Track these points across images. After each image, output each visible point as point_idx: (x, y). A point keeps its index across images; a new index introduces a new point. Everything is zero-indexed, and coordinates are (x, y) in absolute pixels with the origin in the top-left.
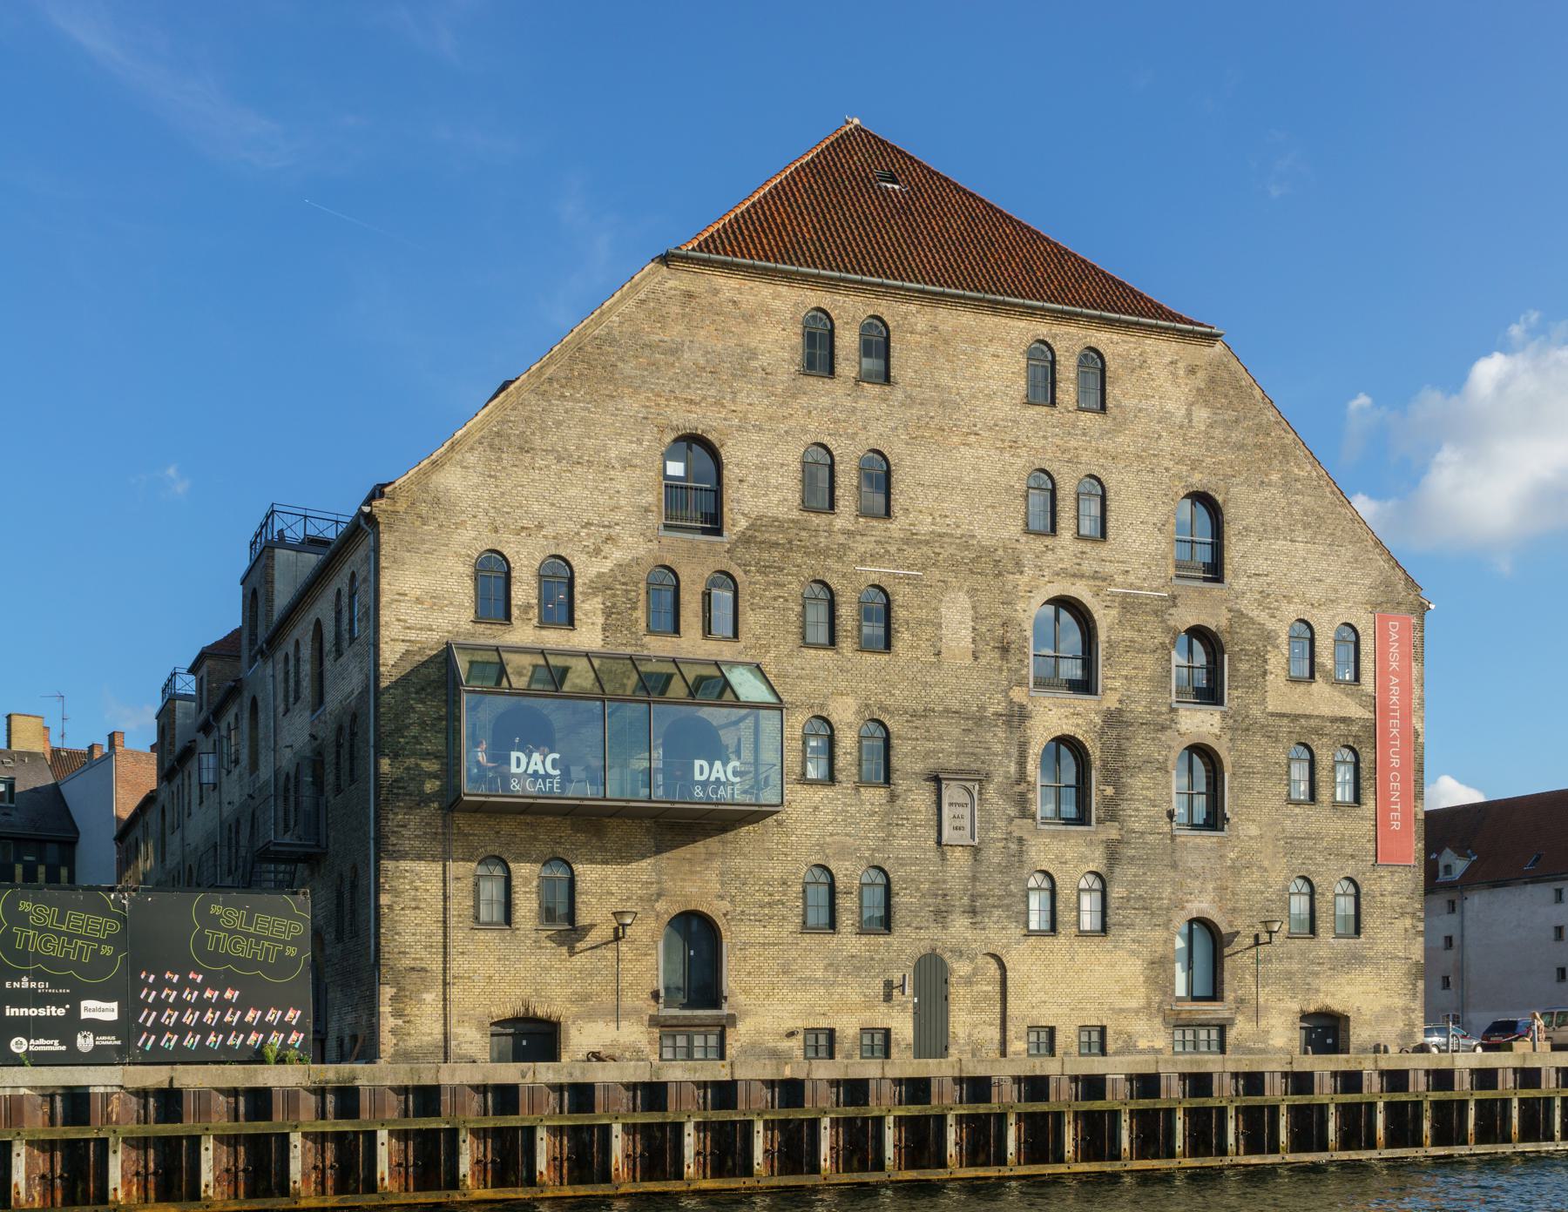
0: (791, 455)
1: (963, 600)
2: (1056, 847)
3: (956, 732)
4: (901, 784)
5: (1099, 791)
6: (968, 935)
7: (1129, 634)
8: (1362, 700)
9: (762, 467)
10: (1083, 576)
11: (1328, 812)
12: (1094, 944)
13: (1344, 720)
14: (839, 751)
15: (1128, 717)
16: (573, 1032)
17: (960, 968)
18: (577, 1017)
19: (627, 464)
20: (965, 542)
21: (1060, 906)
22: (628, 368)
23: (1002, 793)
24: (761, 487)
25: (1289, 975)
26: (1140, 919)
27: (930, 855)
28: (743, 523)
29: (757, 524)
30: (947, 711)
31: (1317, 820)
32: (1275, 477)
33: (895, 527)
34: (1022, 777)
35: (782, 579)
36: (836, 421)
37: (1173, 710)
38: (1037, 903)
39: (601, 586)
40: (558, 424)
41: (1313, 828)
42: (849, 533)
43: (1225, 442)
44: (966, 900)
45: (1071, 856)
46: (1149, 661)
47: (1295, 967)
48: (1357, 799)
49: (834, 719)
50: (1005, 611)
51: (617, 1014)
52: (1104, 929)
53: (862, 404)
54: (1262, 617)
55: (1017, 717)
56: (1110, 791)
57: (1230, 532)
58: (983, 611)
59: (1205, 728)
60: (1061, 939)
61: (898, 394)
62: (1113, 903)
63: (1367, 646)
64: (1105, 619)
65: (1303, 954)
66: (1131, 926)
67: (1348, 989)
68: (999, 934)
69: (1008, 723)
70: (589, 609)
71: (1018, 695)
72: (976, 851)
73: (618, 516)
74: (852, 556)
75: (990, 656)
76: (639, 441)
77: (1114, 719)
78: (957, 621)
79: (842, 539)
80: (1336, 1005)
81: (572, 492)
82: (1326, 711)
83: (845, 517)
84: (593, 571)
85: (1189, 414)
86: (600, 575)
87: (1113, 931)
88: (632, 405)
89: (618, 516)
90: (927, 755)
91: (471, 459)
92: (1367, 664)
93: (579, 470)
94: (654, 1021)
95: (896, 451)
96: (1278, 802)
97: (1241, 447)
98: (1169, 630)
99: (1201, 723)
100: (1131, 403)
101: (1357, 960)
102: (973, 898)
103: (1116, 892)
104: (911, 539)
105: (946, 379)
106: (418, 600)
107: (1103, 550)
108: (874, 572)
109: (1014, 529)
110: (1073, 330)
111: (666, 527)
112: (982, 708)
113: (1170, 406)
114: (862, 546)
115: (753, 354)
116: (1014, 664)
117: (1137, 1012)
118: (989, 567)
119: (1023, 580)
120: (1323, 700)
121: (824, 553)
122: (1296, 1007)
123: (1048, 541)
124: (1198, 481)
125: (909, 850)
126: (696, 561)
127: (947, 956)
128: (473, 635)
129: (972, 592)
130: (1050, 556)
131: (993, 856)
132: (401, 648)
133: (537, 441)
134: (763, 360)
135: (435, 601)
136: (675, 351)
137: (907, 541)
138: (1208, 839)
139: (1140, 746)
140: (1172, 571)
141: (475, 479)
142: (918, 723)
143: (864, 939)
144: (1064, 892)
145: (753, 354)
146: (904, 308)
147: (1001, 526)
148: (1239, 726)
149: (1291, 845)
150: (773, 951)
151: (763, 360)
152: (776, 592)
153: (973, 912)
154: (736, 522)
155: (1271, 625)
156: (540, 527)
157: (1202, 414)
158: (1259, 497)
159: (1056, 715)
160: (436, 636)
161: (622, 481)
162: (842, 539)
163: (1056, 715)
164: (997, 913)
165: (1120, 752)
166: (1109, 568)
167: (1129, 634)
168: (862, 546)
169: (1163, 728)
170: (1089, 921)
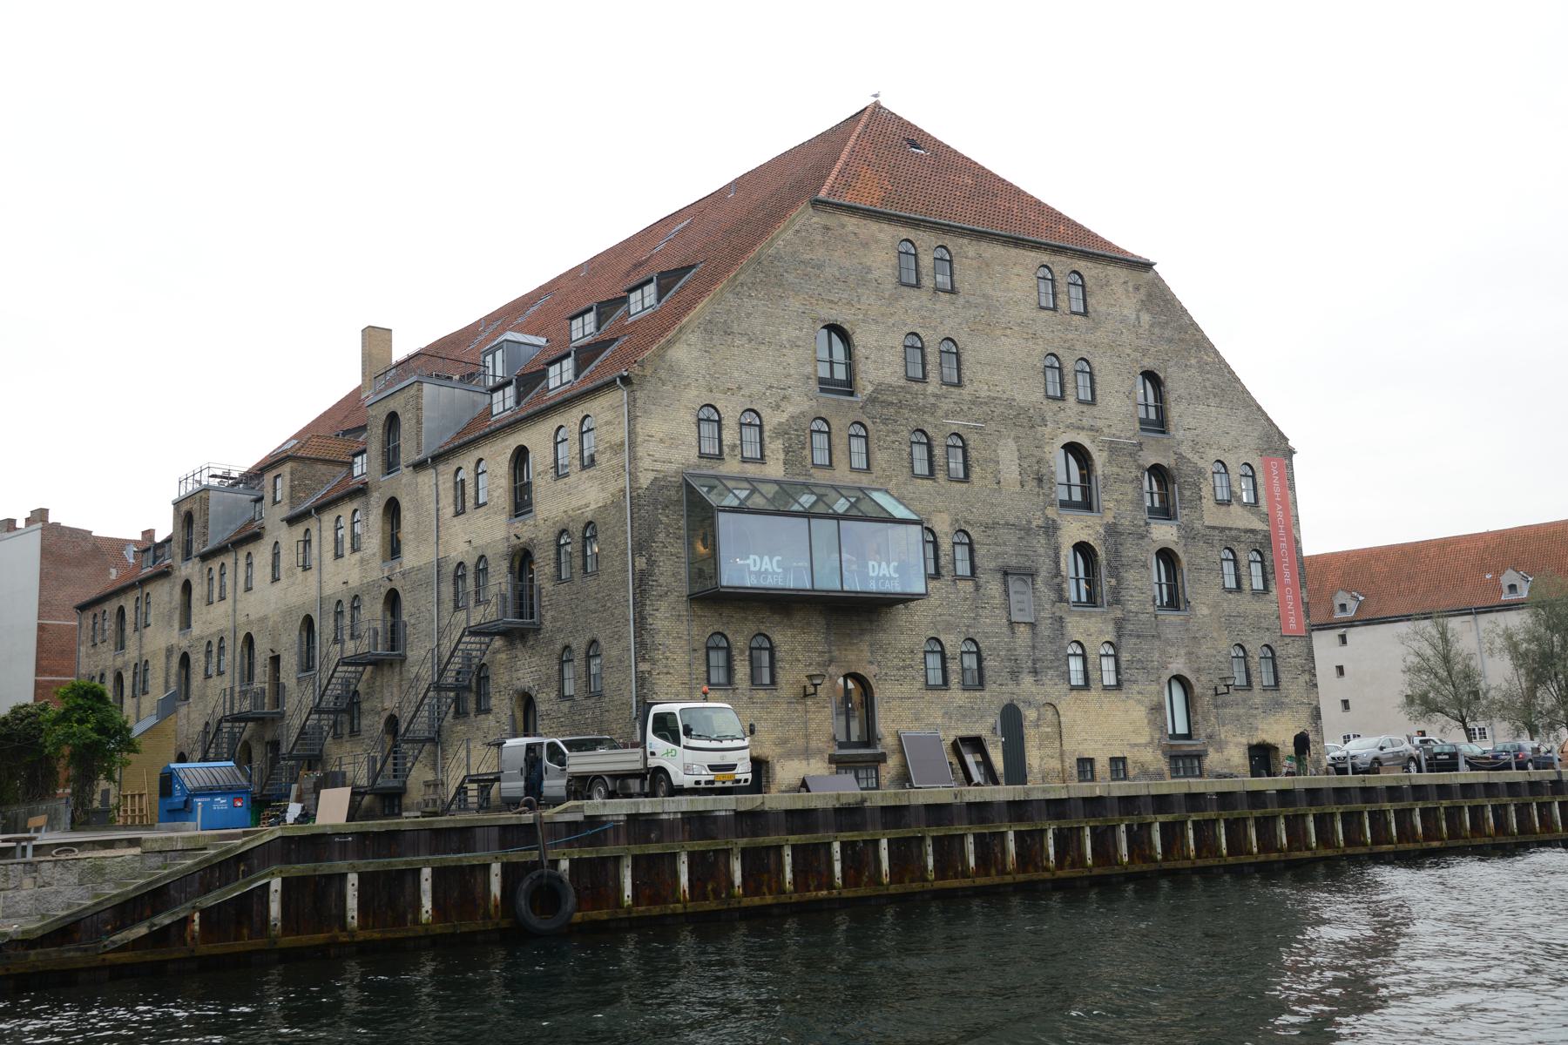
0: (897, 340)
2: (1084, 622)
3: (1014, 540)
4: (983, 578)
5: (1106, 583)
6: (1033, 689)
7: (1115, 470)
8: (1265, 518)
9: (880, 349)
11: (1249, 597)
12: (1113, 696)
13: (1253, 531)
14: (941, 554)
15: (1120, 529)
16: (778, 768)
17: (1030, 715)
18: (781, 756)
19: (794, 345)
20: (1010, 403)
21: (1090, 667)
22: (790, 277)
23: (1046, 584)
24: (880, 366)
25: (1238, 718)
26: (1141, 676)
27: (1005, 629)
28: (870, 388)
30: (1007, 524)
31: (1245, 603)
32: (1193, 361)
33: (966, 392)
34: (1058, 573)
35: (897, 428)
37: (1147, 524)
38: (1075, 665)
39: (781, 432)
40: (749, 315)
41: (1241, 609)
42: (935, 395)
43: (1161, 337)
44: (1030, 664)
45: (1091, 629)
46: (1129, 488)
47: (1242, 711)
48: (1266, 589)
49: (936, 529)
50: (1037, 453)
52: (1119, 685)
53: (938, 306)
54: (1195, 459)
55: (1051, 529)
56: (1113, 582)
57: (1171, 398)
58: (1025, 453)
59: (1168, 537)
60: (1093, 692)
61: (961, 301)
62: (1123, 665)
63: (1260, 479)
64: (1099, 458)
65: (1244, 701)
66: (1135, 682)
67: (1276, 727)
68: (1052, 689)
69: (1046, 533)
70: (775, 448)
71: (1051, 512)
72: (1033, 625)
74: (940, 413)
75: (1031, 484)
76: (801, 329)
77: (1112, 531)
79: (932, 400)
80: (1270, 739)
81: (759, 364)
82: (1240, 524)
83: (933, 386)
84: (776, 421)
85: (1138, 318)
86: (780, 424)
87: (1126, 685)
88: (795, 304)
89: (790, 382)
90: (997, 556)
91: (693, 338)
92: (1261, 492)
93: (763, 348)
94: (833, 759)
95: (962, 339)
96: (1218, 590)
97: (1170, 341)
98: (1139, 467)
99: (1164, 533)
100: (1102, 309)
101: (1278, 705)
102: (1034, 662)
103: (1125, 657)
104: (975, 401)
105: (991, 292)
106: (662, 441)
107: (1095, 411)
108: (955, 424)
109: (1038, 395)
110: (1063, 259)
111: (822, 390)
112: (1029, 522)
113: (1126, 312)
114: (946, 405)
115: (869, 270)
116: (1046, 491)
117: (1146, 745)
118: (1025, 421)
119: (1047, 430)
120: (1238, 518)
121: (921, 410)
122: (1244, 741)
123: (1060, 404)
124: (1149, 364)
125: (990, 625)
126: (842, 414)
127: (1021, 705)
128: (699, 467)
130: (1062, 414)
131: (1045, 630)
132: (651, 475)
133: (735, 328)
134: (876, 274)
135: (672, 441)
138: (1171, 617)
139: (1130, 550)
140: (1138, 426)
141: (696, 354)
142: (990, 532)
143: (967, 694)
144: (1091, 657)
145: (869, 270)
146: (960, 241)
147: (1029, 394)
148: (1189, 535)
149: (1229, 621)
151: (876, 274)
152: (893, 437)
153: (1035, 672)
154: (865, 388)
155: (1201, 464)
156: (740, 388)
157: (1146, 318)
158: (1185, 375)
159: (1076, 528)
160: (674, 467)
161: (791, 357)
162: (932, 400)
163: (1076, 528)
164: (1050, 672)
166: (1099, 424)
167: (1115, 470)
168: (946, 405)
169: (1142, 537)
170: (1109, 679)
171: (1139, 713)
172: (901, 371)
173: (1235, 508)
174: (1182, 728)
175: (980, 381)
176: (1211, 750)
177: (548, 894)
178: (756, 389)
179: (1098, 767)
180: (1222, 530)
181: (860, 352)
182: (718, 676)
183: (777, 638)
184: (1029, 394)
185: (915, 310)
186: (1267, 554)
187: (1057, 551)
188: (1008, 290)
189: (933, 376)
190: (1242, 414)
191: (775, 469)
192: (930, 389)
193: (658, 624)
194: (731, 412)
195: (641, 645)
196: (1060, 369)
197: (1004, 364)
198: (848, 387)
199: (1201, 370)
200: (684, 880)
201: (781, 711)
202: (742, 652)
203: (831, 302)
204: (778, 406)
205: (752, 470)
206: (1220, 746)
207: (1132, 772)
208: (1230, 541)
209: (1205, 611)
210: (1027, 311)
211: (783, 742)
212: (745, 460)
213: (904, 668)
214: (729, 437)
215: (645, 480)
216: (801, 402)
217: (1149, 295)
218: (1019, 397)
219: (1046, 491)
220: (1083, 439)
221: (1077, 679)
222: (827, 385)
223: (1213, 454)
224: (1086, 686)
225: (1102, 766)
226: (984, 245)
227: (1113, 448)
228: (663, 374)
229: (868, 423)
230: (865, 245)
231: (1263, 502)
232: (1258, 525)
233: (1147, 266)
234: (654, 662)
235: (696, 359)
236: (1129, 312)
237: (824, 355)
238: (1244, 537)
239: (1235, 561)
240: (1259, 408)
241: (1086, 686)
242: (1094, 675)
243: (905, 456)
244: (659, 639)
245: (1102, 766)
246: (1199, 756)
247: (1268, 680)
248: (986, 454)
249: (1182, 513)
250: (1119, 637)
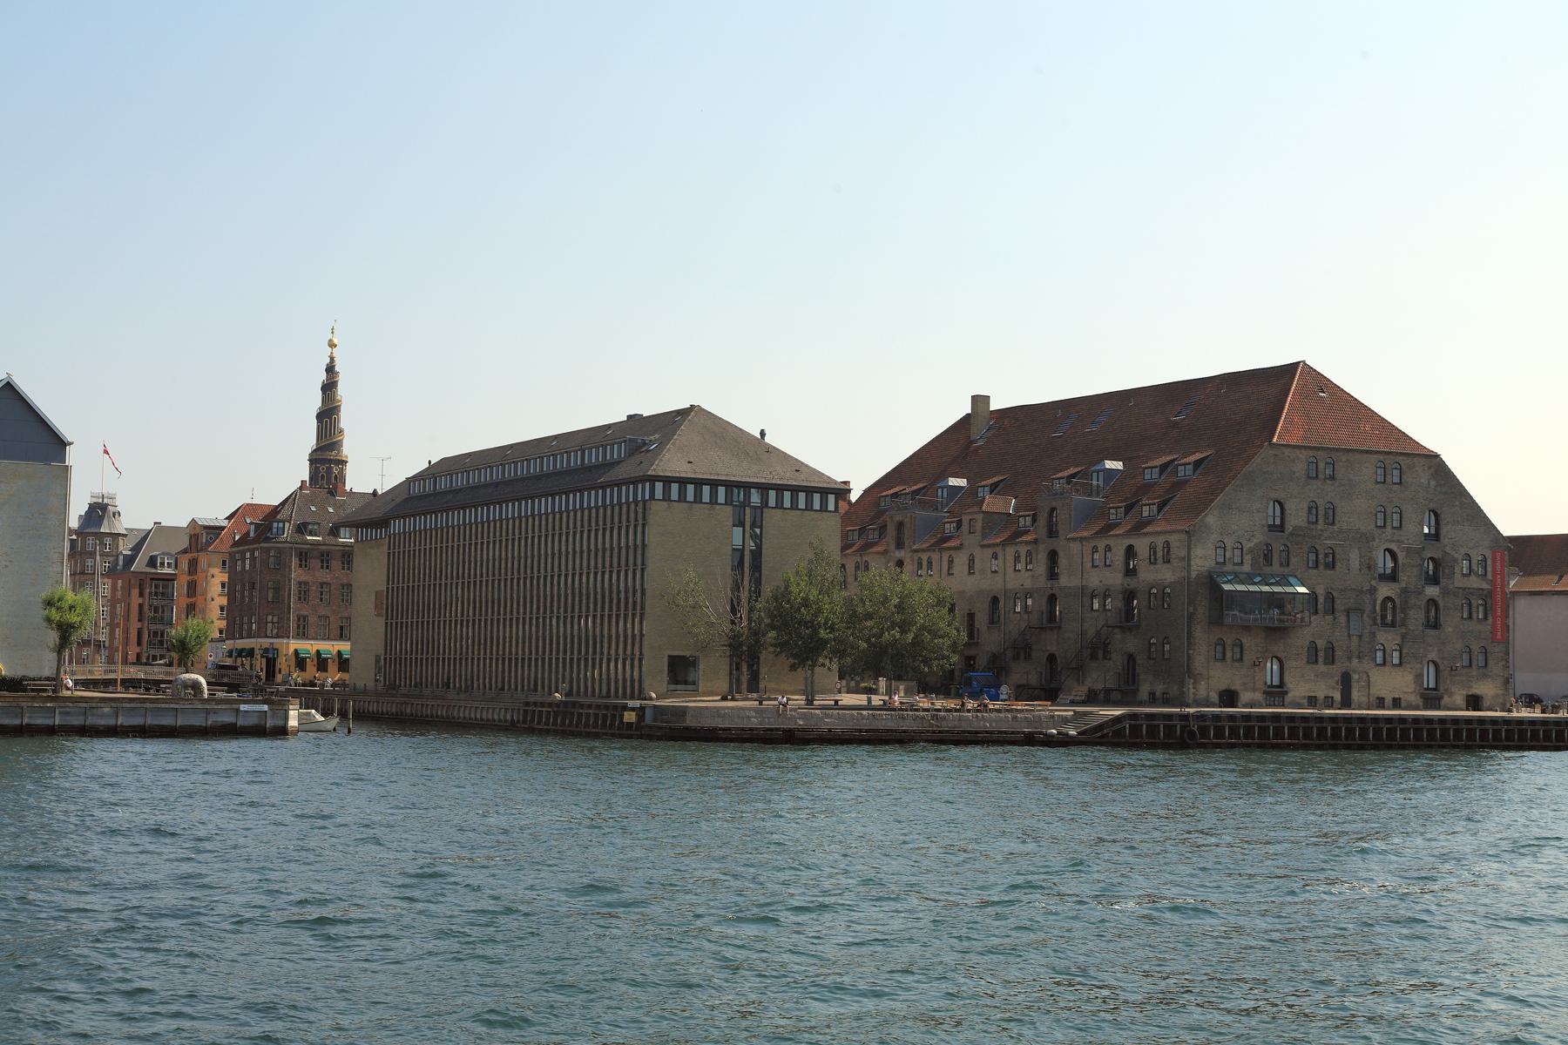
0: (1305, 505)
5: (1400, 616)
17: (1355, 677)
24: (1297, 518)
29: (1296, 528)
38: (1379, 654)
39: (1251, 551)
48: (1486, 618)
51: (1254, 690)
55: (1373, 591)
57: (1443, 523)
63: (1489, 562)
64: (1401, 556)
68: (1367, 665)
70: (1247, 558)
72: (1360, 637)
77: (1405, 591)
78: (1355, 558)
92: (1489, 569)
99: (1432, 591)
101: (1485, 676)
104: (1341, 531)
118: (1364, 539)
120: (1474, 582)
124: (1432, 506)
131: (1366, 638)
139: (1413, 600)
148: (1445, 592)
154: (1289, 528)
157: (1433, 483)
163: (1385, 590)
170: (1396, 661)
171: (1410, 678)
173: (1473, 578)
177: (1192, 734)
181: (1288, 512)
182: (1219, 656)
183: (1244, 640)
189: (1321, 520)
191: (1247, 568)
194: (1229, 543)
195: (1189, 643)
197: (1356, 513)
198: (1281, 528)
205: (1237, 568)
206: (1451, 695)
208: (1467, 594)
214: (1228, 554)
215: (1194, 575)
216: (1260, 538)
220: (1393, 547)
221: (1379, 660)
222: (1272, 528)
223: (1463, 551)
224: (1384, 664)
225: (1388, 701)
227: (1408, 550)
231: (1490, 576)
232: (1485, 586)
233: (1437, 456)
237: (1273, 512)
239: (1470, 605)
241: (1384, 664)
245: (1388, 701)
246: (1440, 698)
247: (1482, 663)
249: (1443, 581)
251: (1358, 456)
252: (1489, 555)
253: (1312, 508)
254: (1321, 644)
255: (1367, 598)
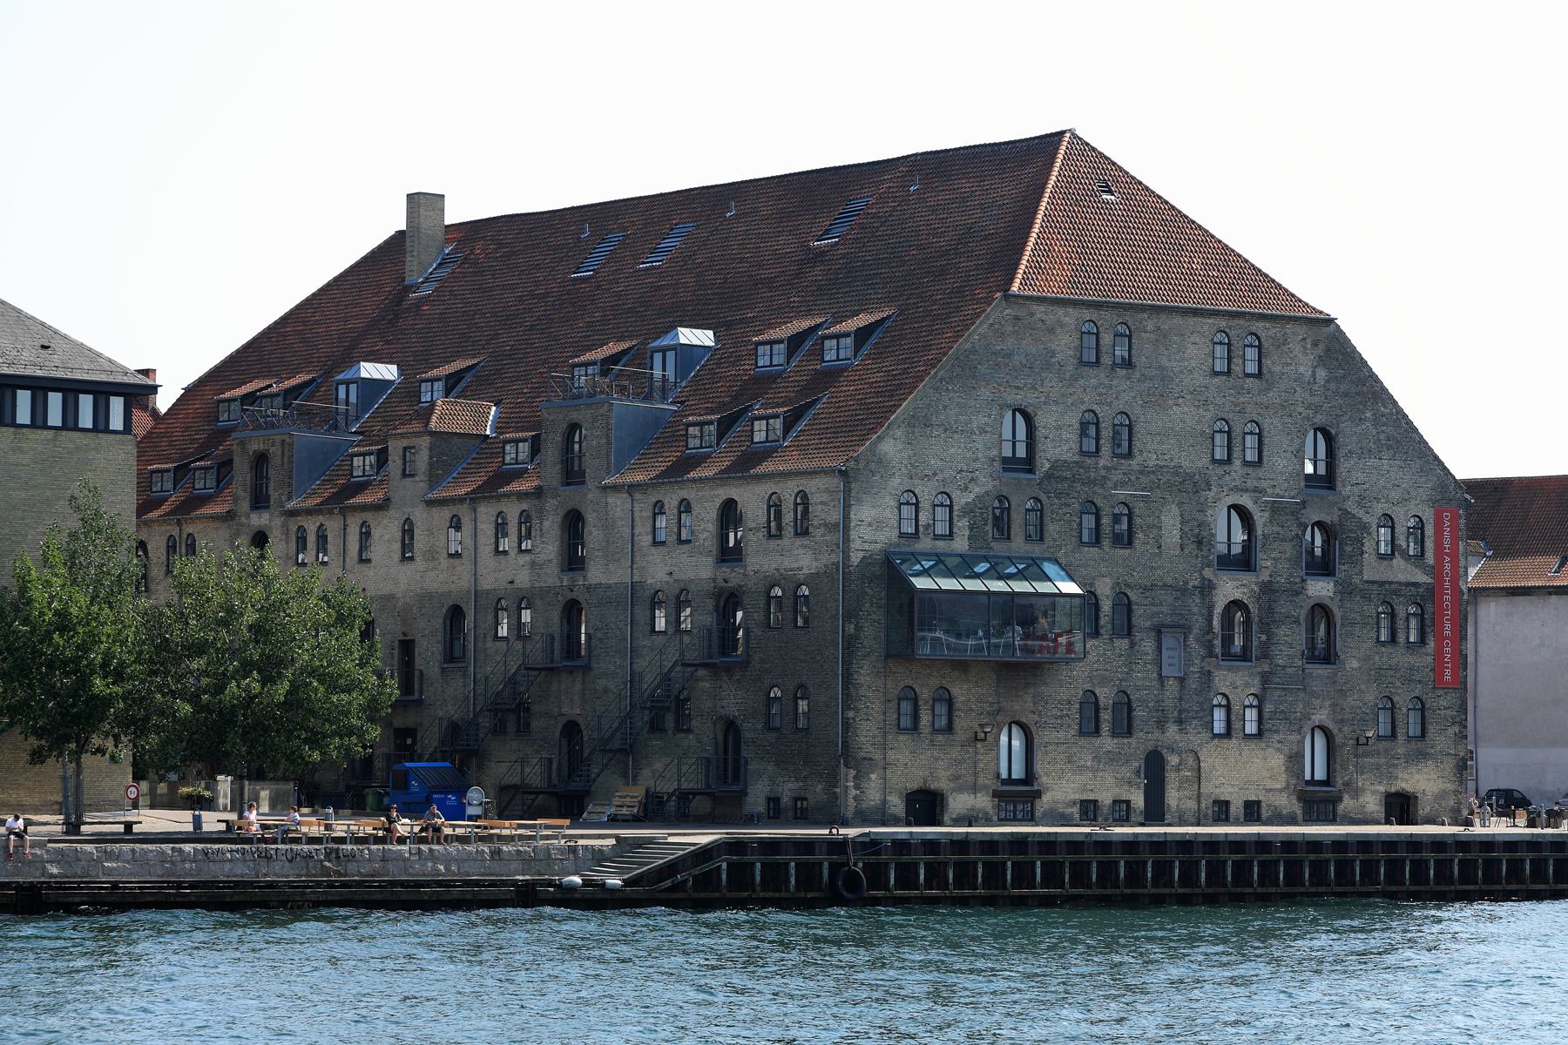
1: (1175, 510)
3: (1170, 600)
10: (1247, 491)
19: (983, 431)
21: (1233, 718)
23: (1197, 640)
36: (1100, 395)
37: (1304, 581)
39: (968, 510)
40: (945, 407)
42: (1106, 468)
50: (1199, 516)
53: (1115, 382)
54: (1360, 513)
55: (1207, 588)
58: (1187, 517)
62: (1266, 716)
70: (962, 525)
71: (1208, 573)
72: (1182, 680)
73: (978, 465)
74: (1110, 484)
81: (953, 451)
82: (1402, 578)
85: (1314, 374)
88: (985, 393)
89: (978, 465)
102: (1180, 712)
105: (1165, 363)
106: (870, 525)
113: (1301, 370)
116: (1205, 553)
129: (1180, 504)
130: (1227, 478)
131: (1193, 684)
134: (1059, 357)
136: (1009, 356)
137: (1141, 472)
145: (1053, 354)
150: (1062, 748)
151: (1059, 357)
153: (1180, 722)
155: (1366, 518)
156: (935, 474)
157: (1322, 374)
160: (879, 546)
162: (1103, 473)
165: (1270, 610)
166: (1264, 484)
167: (1276, 529)
169: (1298, 593)
171: (1277, 761)
172: (1076, 447)
173: (1398, 562)
174: (1320, 775)
175: (1150, 452)
176: (1346, 796)
178: (949, 473)
179: (1233, 809)
180: (1382, 584)
181: (1041, 432)
184: (1193, 460)
185: (1093, 390)
186: (1429, 608)
187: (1210, 609)
188: (1184, 359)
189: (1106, 449)
190: (1417, 464)
192: (1102, 462)
193: (862, 680)
194: (926, 493)
195: (847, 697)
196: (1229, 433)
198: (1028, 464)
199: (1376, 422)
200: (922, 877)
201: (955, 752)
202: (926, 703)
203: (1018, 388)
204: (966, 488)
205: (941, 545)
206: (1357, 793)
207: (1265, 814)
209: (1355, 664)
210: (1200, 379)
211: (957, 778)
212: (937, 537)
213: (1061, 717)
214: (924, 518)
215: (855, 558)
216: (985, 484)
217: (1328, 350)
218: (1186, 464)
219: (1205, 553)
220: (1246, 501)
221: (1219, 727)
222: (1010, 464)
223: (1379, 508)
224: (1228, 734)
225: (1236, 808)
226: (1163, 316)
227: (1276, 509)
228: (873, 466)
229: (1044, 498)
230: (1051, 330)
231: (1430, 557)
232: (1421, 578)
233: (1330, 321)
234: (857, 710)
235: (900, 451)
236: (1305, 371)
238: (1404, 590)
240: (1436, 458)
241: (1228, 734)
242: (1236, 725)
243: (1075, 526)
244: (862, 692)
245: (1236, 808)
246: (1336, 800)
247: (1414, 730)
248: (1150, 520)
249: (1342, 569)
250: (1264, 689)
251: (1177, 320)
252: (1428, 515)
253: (1089, 426)
254: (1105, 695)
255: (1195, 604)
